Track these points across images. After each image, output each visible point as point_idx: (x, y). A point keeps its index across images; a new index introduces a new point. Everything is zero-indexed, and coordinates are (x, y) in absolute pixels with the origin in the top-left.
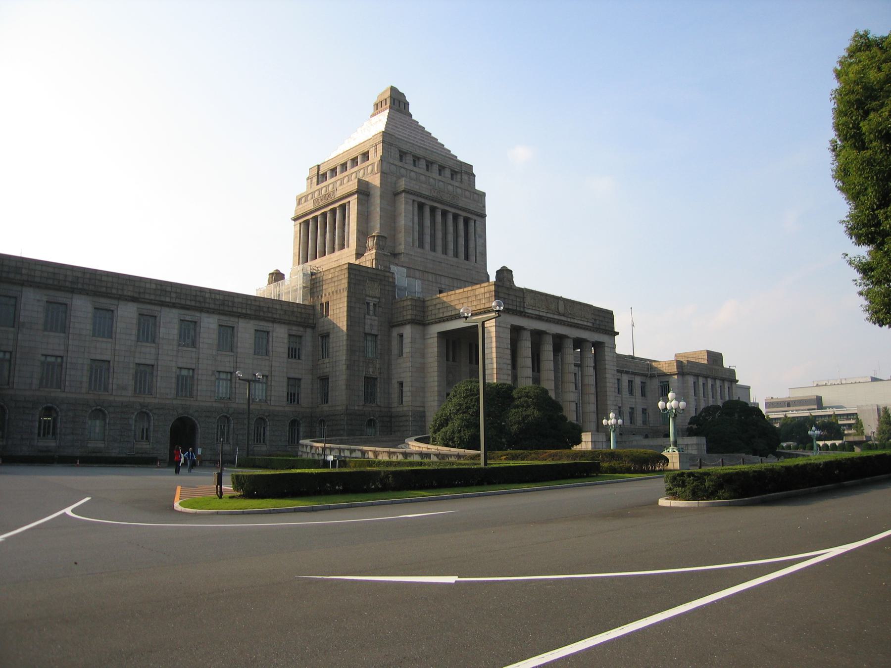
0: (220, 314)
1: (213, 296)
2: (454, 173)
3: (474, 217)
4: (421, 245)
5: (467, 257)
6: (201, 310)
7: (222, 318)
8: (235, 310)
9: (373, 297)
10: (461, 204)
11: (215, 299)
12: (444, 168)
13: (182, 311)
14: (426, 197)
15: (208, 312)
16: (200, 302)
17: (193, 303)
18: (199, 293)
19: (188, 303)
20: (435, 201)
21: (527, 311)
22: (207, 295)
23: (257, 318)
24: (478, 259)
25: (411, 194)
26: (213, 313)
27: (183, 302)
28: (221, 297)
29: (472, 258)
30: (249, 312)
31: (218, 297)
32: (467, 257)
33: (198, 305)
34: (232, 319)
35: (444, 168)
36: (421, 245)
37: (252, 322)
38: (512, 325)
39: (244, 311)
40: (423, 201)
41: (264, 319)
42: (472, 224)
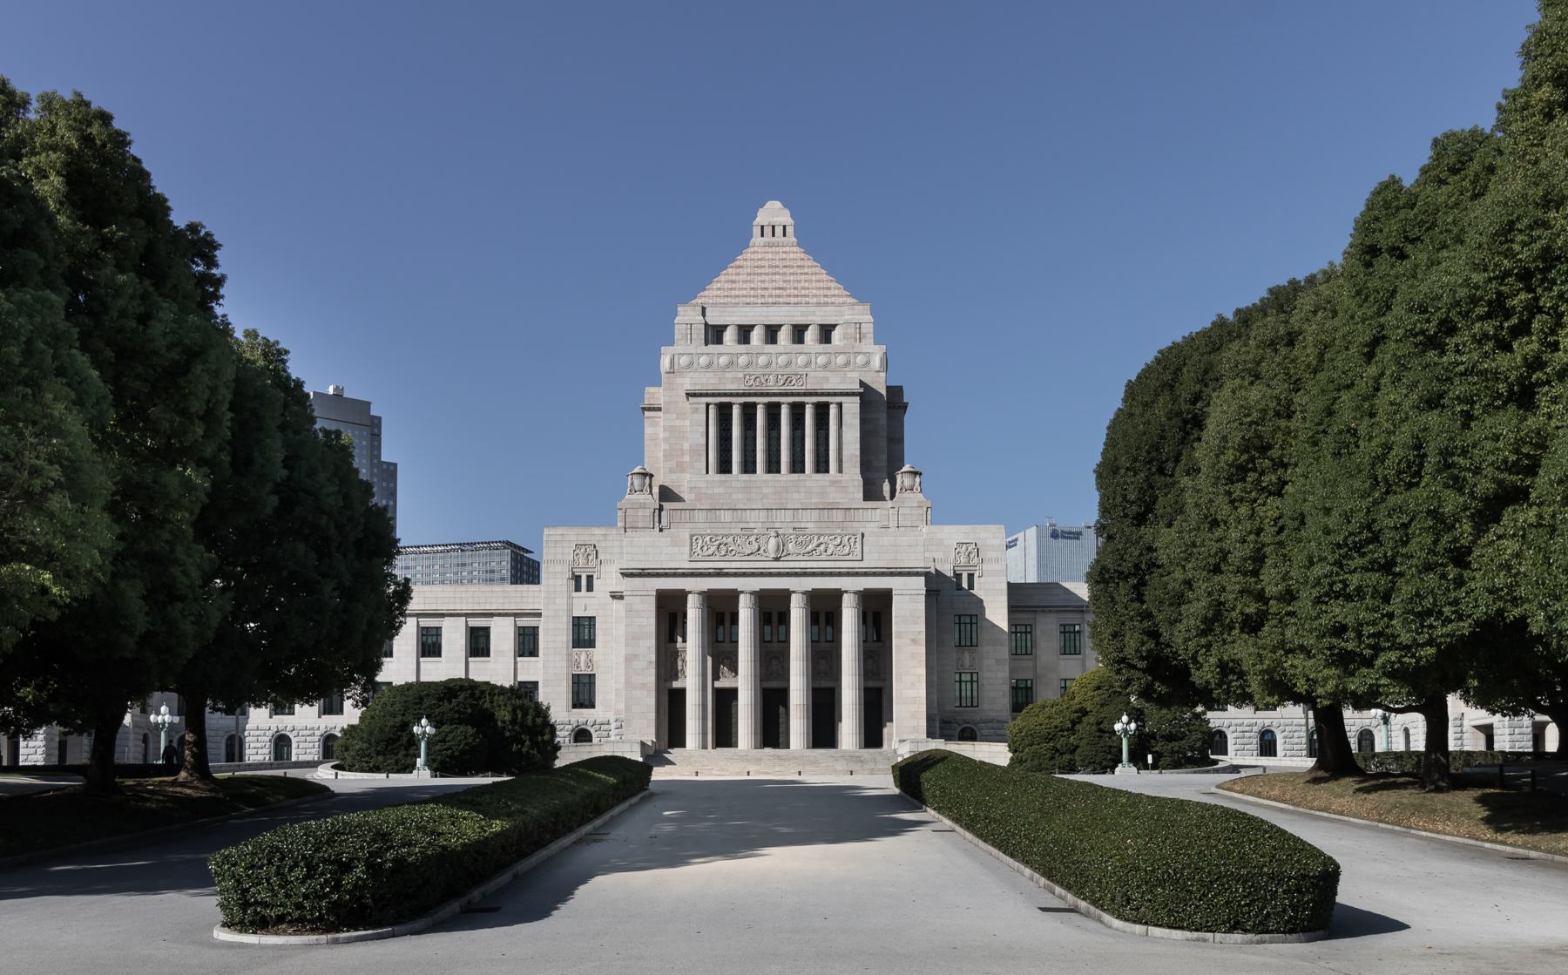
3: (838, 399)
4: (724, 467)
5: (822, 466)
10: (810, 386)
25: (701, 395)
36: (724, 467)
42: (833, 411)
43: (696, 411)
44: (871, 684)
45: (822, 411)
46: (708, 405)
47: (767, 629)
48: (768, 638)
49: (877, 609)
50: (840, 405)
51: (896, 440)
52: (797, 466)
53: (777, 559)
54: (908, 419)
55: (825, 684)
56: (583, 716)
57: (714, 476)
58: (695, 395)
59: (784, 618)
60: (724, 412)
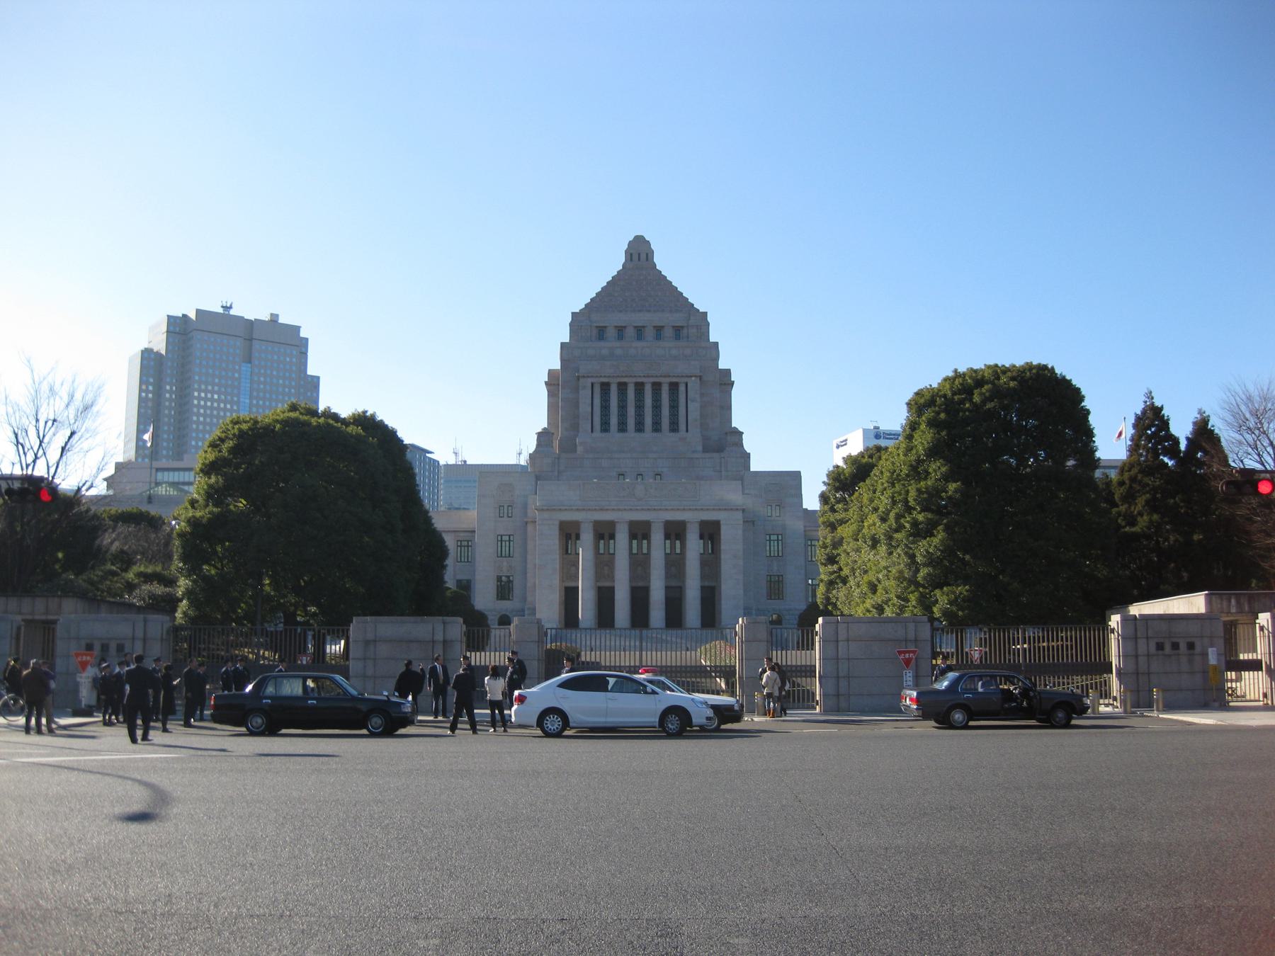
3: (686, 380)
4: (605, 427)
5: (674, 427)
29: (682, 426)
32: (674, 427)
36: (605, 427)
42: (682, 388)
43: (584, 388)
44: (707, 584)
45: (674, 387)
47: (635, 542)
48: (635, 551)
49: (710, 532)
51: (729, 407)
52: (657, 427)
54: (736, 393)
55: (674, 583)
56: (505, 605)
57: (597, 434)
59: (646, 536)
60: (605, 387)
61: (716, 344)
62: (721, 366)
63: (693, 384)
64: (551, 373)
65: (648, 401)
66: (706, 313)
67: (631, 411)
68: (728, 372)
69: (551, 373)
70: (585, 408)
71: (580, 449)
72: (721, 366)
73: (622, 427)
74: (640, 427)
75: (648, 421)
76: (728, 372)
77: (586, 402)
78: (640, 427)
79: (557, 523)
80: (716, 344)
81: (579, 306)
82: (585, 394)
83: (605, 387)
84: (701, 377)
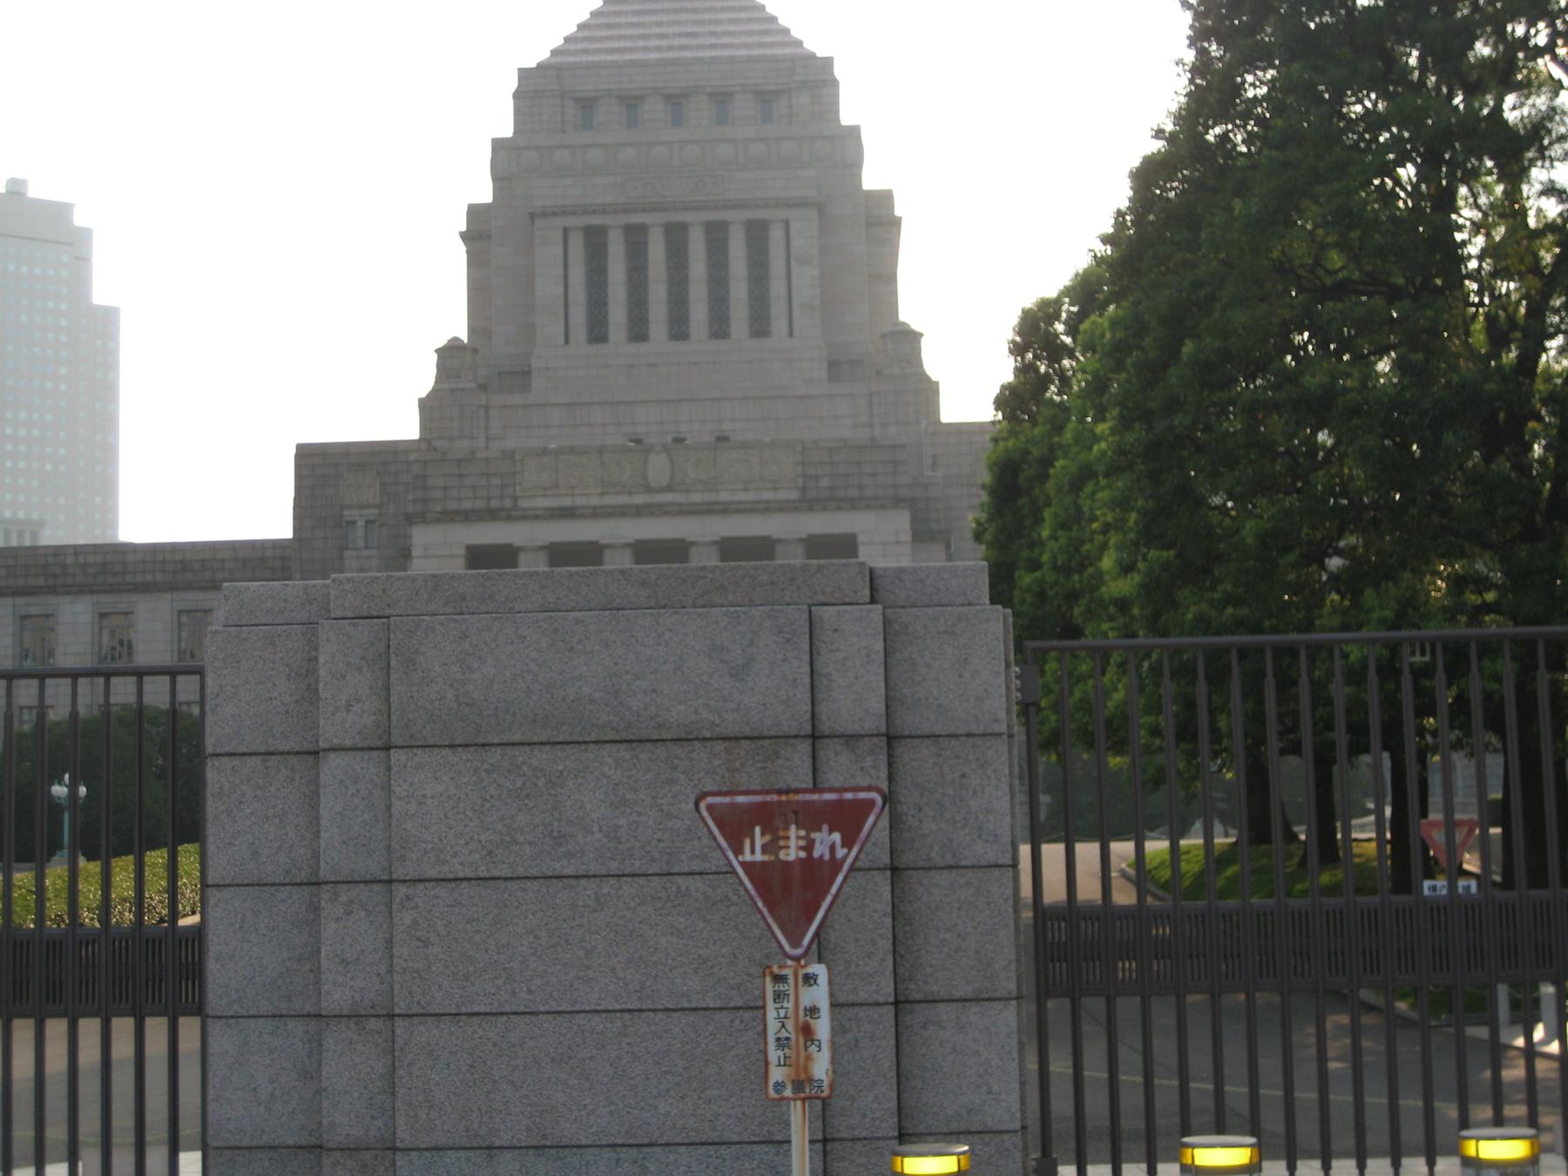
0: (92, 592)
1: (81, 559)
2: (766, 99)
3: (783, 214)
4: (598, 332)
5: (760, 327)
6: (52, 590)
7: (103, 598)
8: (129, 578)
9: (362, 507)
11: (85, 566)
12: (730, 95)
13: (20, 601)
14: (604, 210)
15: (67, 593)
16: (55, 576)
17: (41, 581)
18: (51, 560)
19: (31, 582)
20: (635, 211)
21: (524, 504)
22: (69, 560)
23: (172, 588)
24: (796, 324)
25: (554, 214)
26: (80, 592)
27: (21, 582)
28: (99, 559)
29: (779, 325)
30: (159, 577)
31: (91, 559)
33: (51, 582)
34: (125, 598)
35: (730, 95)
36: (598, 332)
37: (168, 596)
38: (468, 548)
39: (148, 578)
40: (596, 220)
41: (189, 587)
42: (776, 234)
45: (757, 234)
46: (566, 231)
50: (787, 224)
51: (888, 279)
53: (669, 488)
58: (544, 214)
60: (595, 240)
61: (854, 132)
62: (871, 180)
63: (804, 230)
64: (475, 212)
65: (698, 269)
66: (828, 63)
67: (658, 293)
68: (885, 198)
69: (475, 212)
70: (548, 288)
71: (537, 382)
72: (871, 180)
73: (638, 333)
74: (679, 330)
75: (699, 311)
76: (885, 198)
77: (554, 272)
78: (679, 330)
79: (463, 551)
80: (854, 132)
81: (536, 53)
82: (548, 255)
83: (595, 240)
84: (821, 208)
